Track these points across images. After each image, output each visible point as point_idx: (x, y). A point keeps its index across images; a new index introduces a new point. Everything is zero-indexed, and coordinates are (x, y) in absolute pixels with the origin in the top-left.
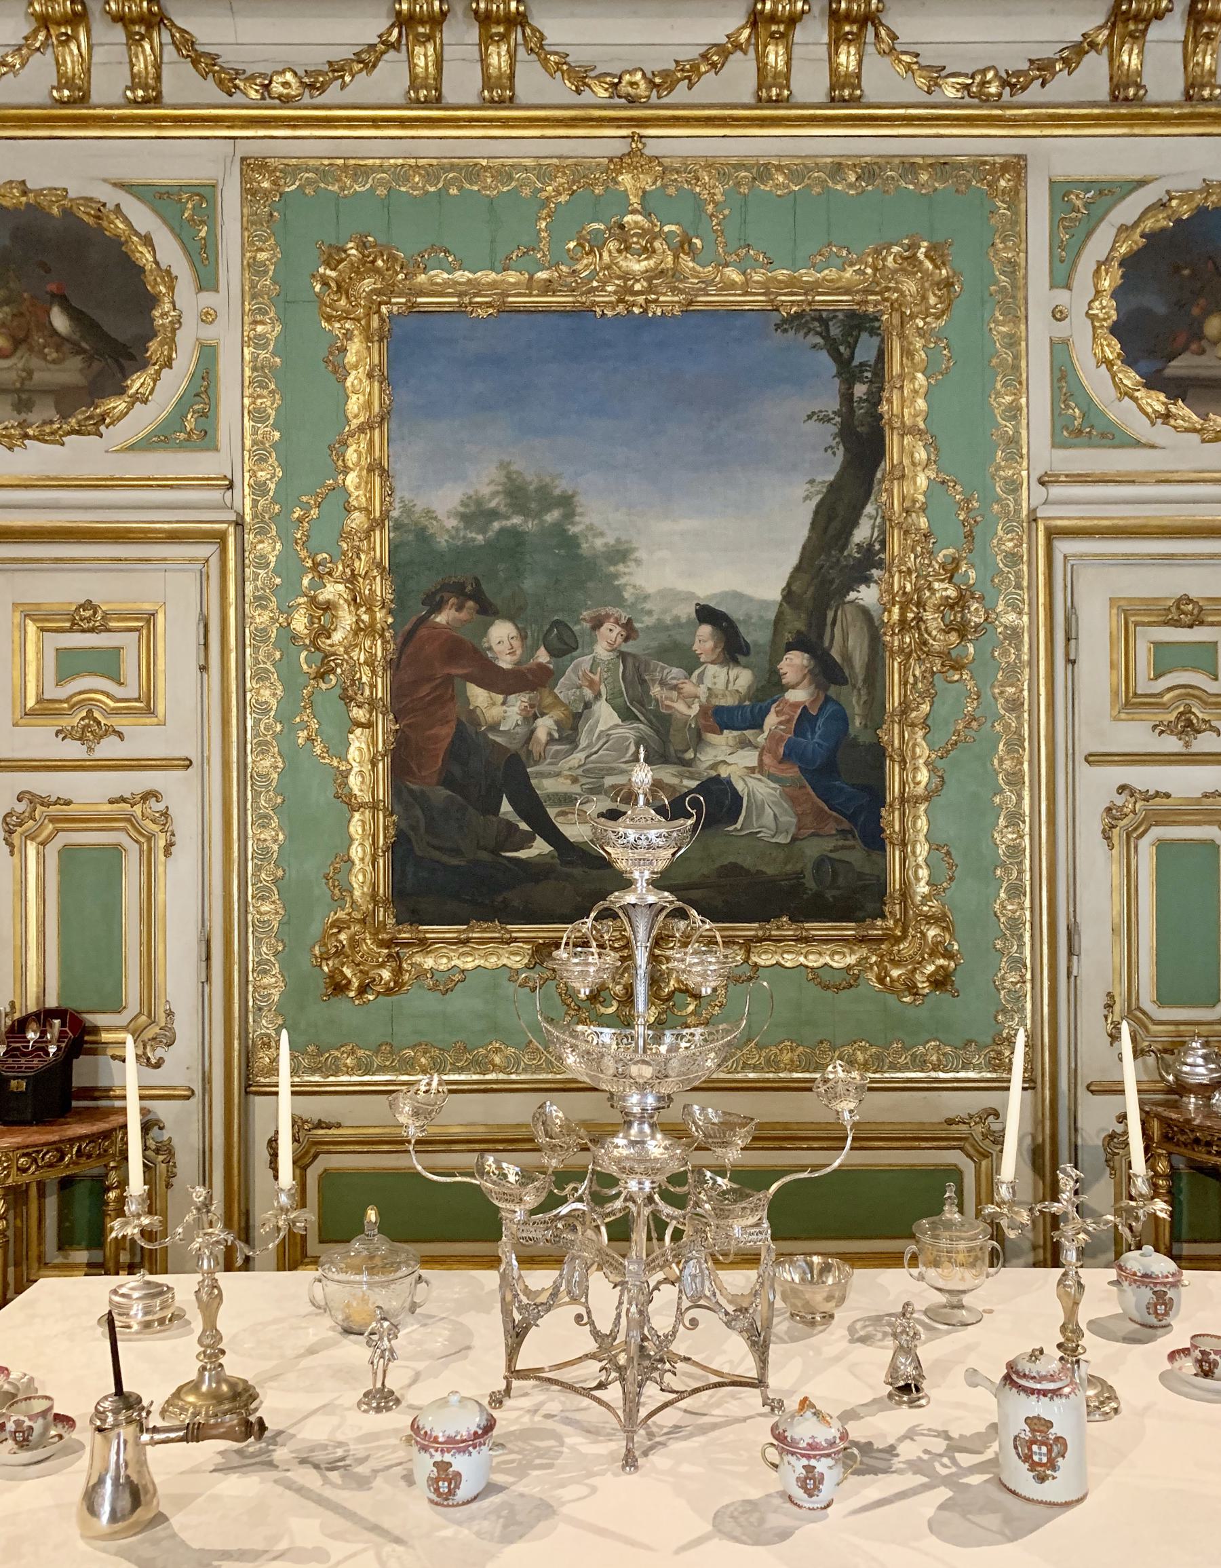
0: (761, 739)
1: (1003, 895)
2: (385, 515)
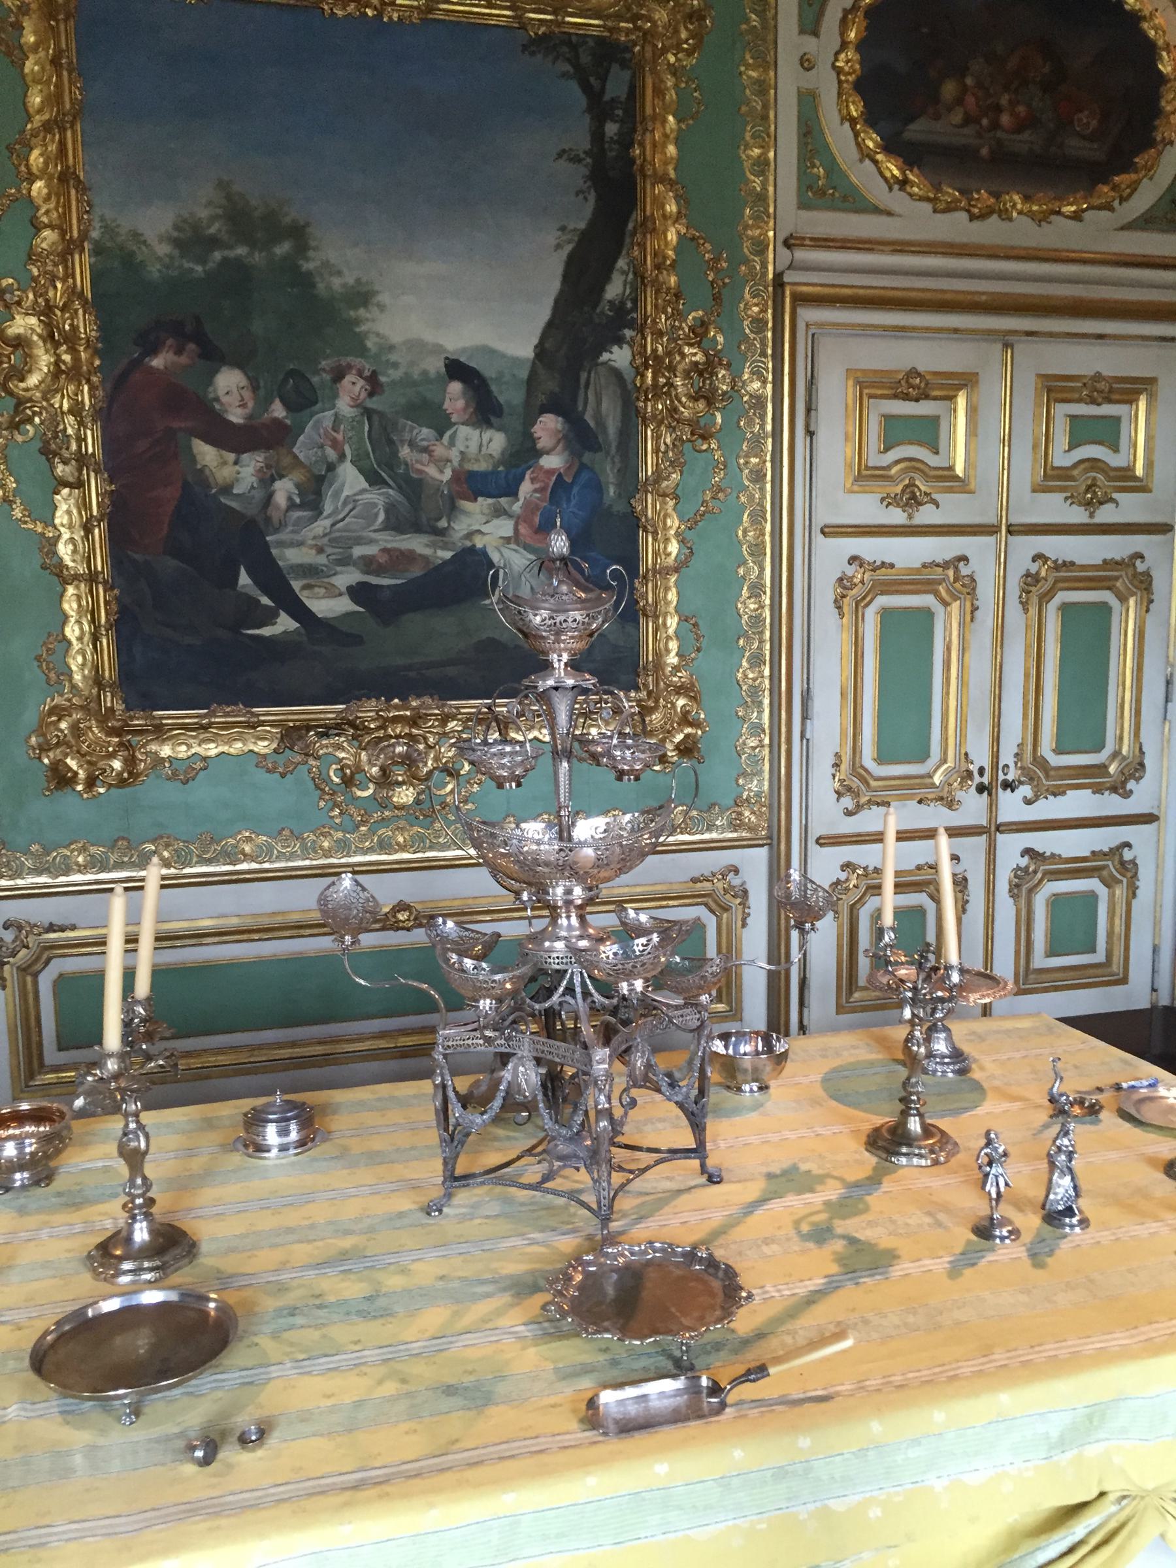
0: (517, 507)
1: (745, 664)
2: (84, 235)
